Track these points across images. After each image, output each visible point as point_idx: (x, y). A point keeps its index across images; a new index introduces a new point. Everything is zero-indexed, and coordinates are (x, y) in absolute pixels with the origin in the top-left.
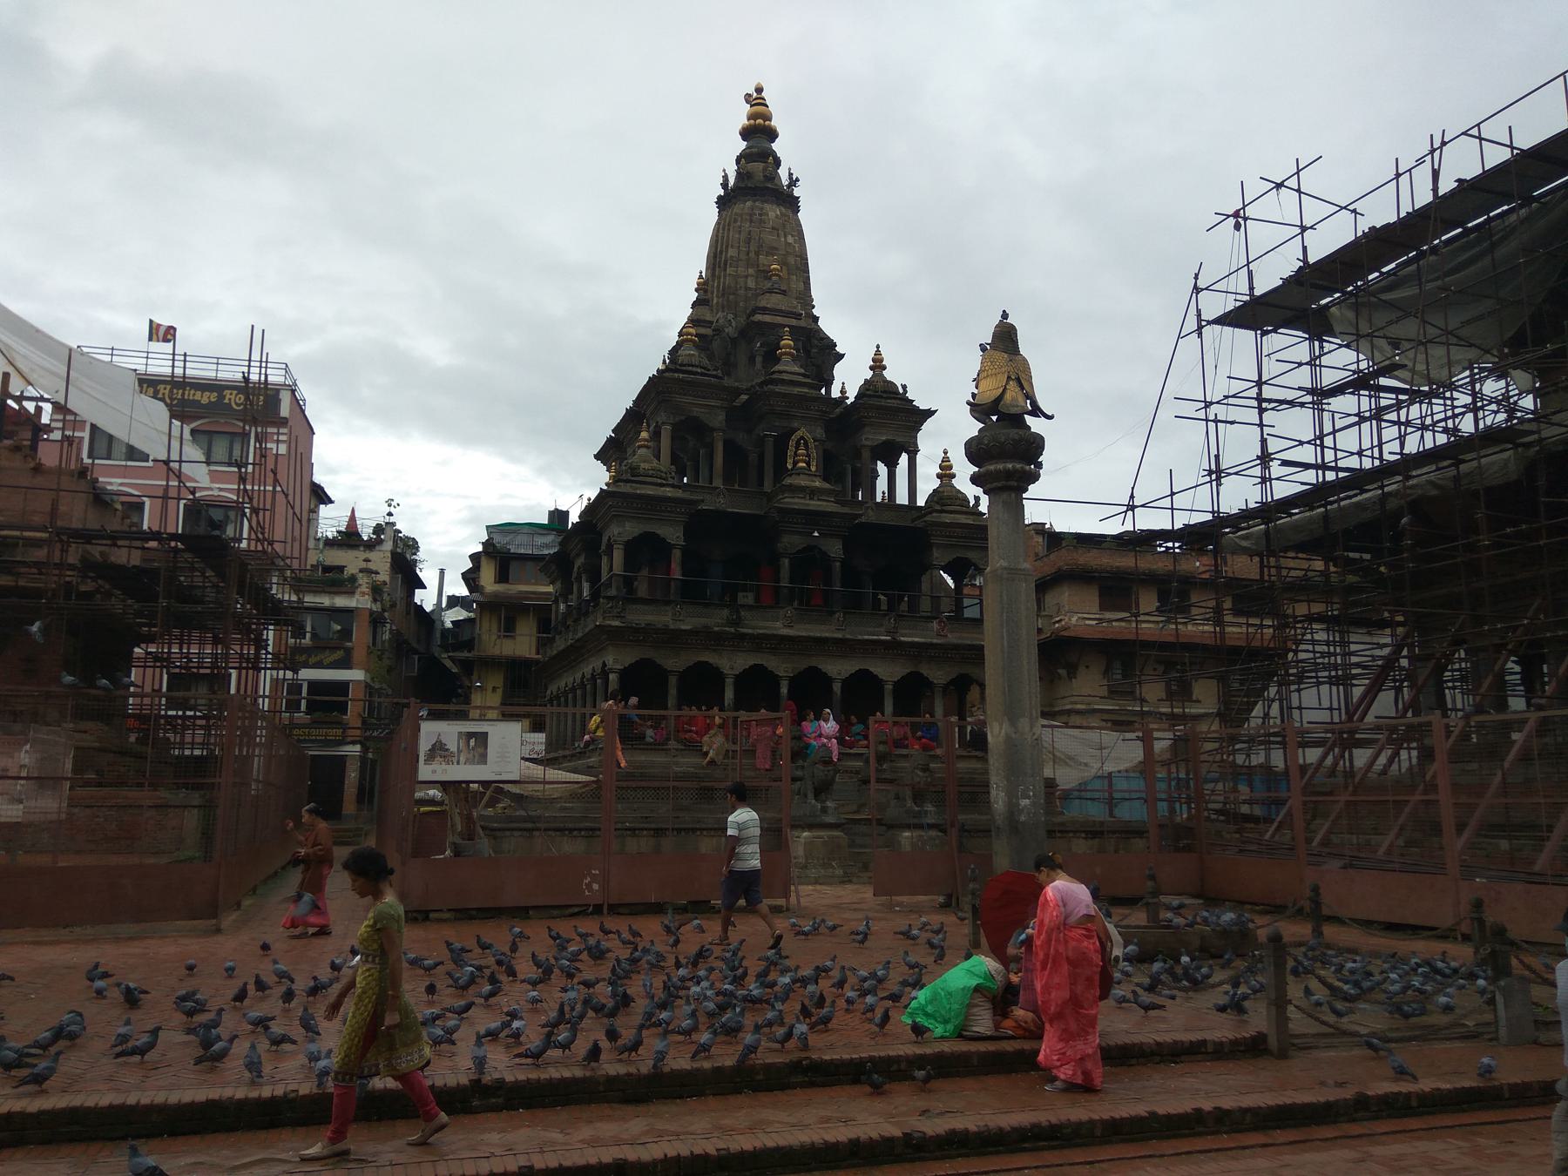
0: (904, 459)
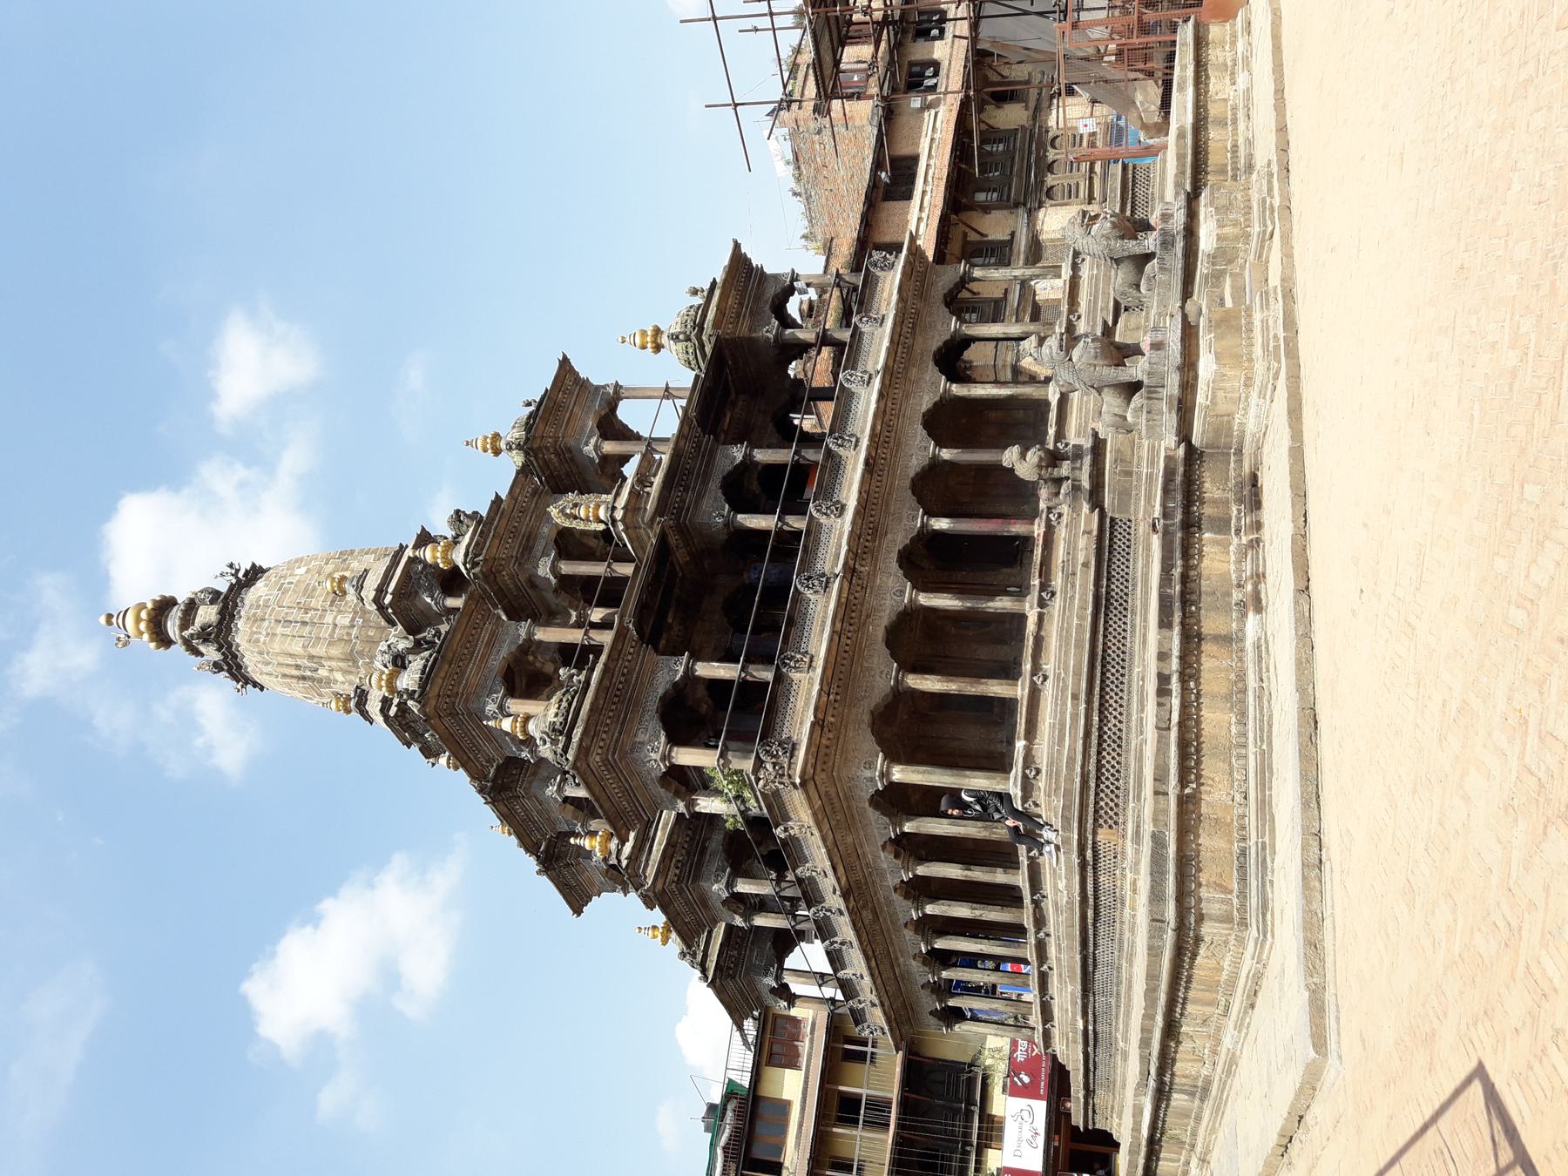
0: (628, 413)
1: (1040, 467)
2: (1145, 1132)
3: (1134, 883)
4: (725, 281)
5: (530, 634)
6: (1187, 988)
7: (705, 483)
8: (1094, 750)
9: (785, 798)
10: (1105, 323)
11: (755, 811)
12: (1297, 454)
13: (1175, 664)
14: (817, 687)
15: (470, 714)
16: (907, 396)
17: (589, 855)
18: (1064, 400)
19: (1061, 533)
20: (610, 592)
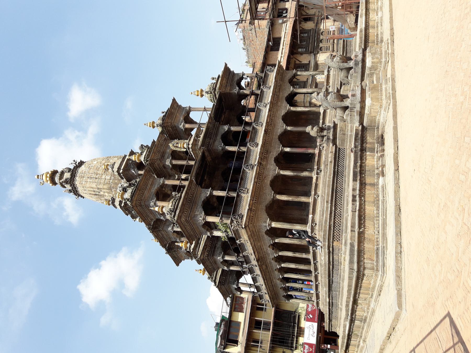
0: (193, 115)
1: (317, 132)
3: (345, 258)
4: (222, 75)
5: (164, 182)
6: (360, 289)
7: (216, 136)
8: (333, 218)
9: (240, 231)
10: (338, 88)
11: (231, 235)
12: (395, 128)
13: (358, 192)
14: (249, 198)
15: (146, 206)
16: (277, 110)
17: (181, 248)
18: (325, 112)
19: (324, 152)
20: (188, 170)
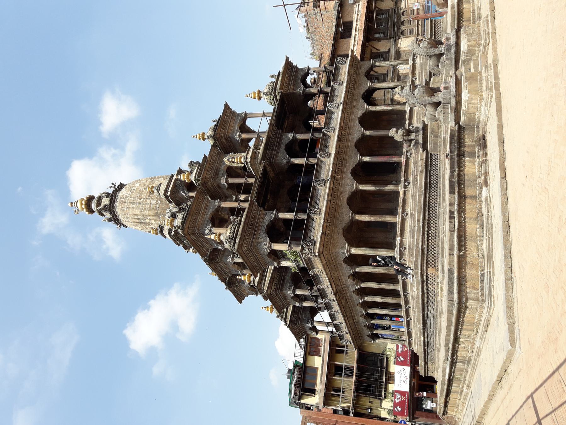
0: (251, 123)
1: (403, 136)
2: (447, 377)
3: (442, 287)
4: (283, 72)
5: (219, 205)
6: (462, 325)
7: (279, 147)
8: (426, 240)
9: (313, 260)
10: (426, 80)
11: (302, 265)
12: (500, 126)
13: (456, 207)
14: (322, 220)
15: (200, 234)
16: (352, 111)
18: (411, 110)
19: (412, 160)
20: (247, 189)
